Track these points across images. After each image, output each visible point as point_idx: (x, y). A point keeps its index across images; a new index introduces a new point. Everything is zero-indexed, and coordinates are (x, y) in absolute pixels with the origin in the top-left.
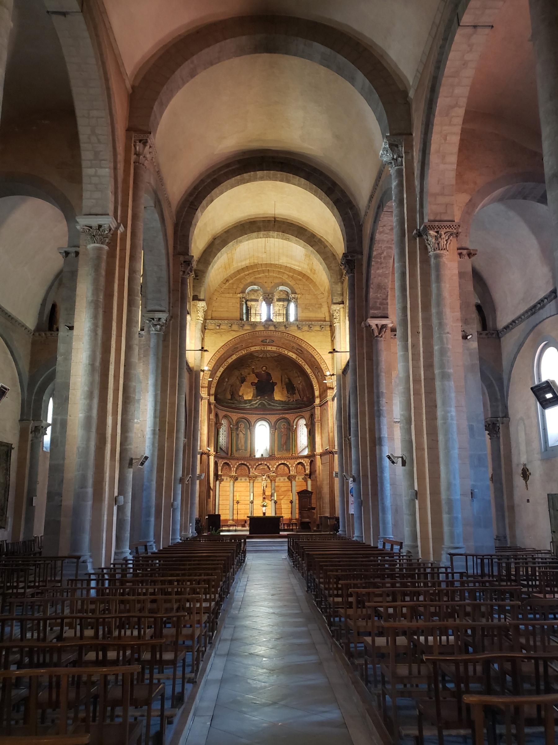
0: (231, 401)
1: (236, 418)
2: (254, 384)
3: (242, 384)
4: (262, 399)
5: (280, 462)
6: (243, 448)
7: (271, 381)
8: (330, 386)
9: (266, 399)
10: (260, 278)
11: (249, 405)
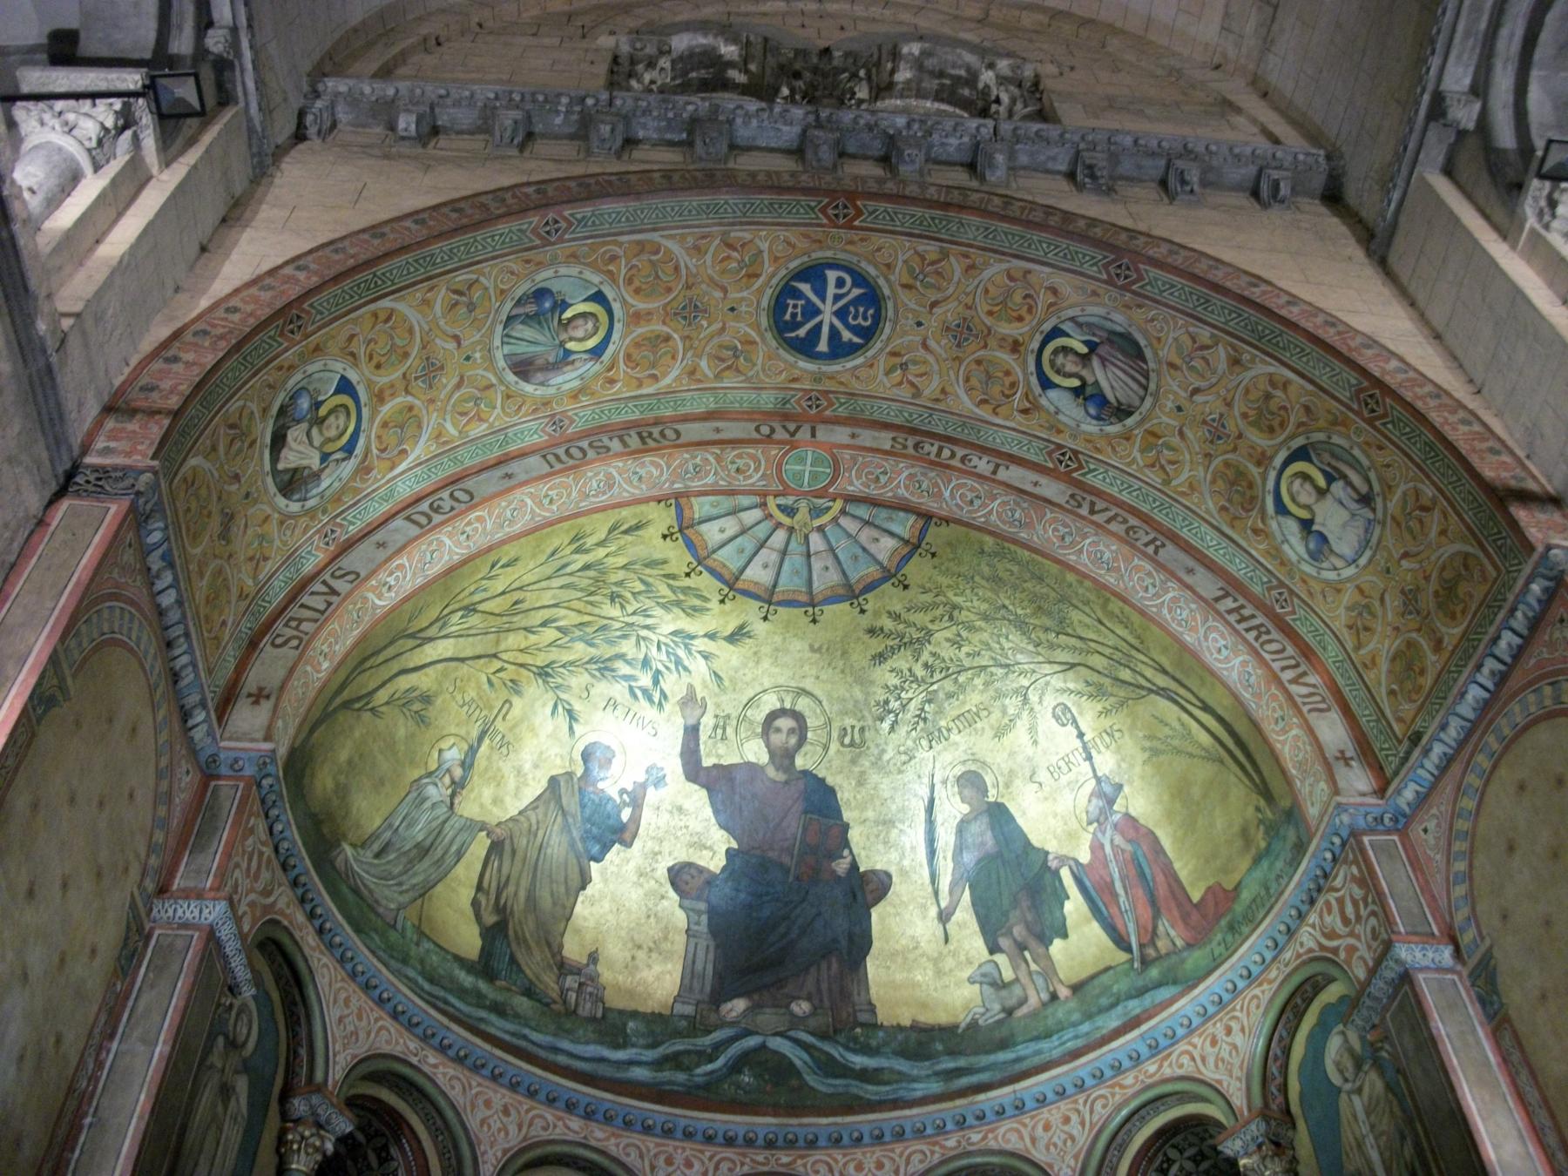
0: (483, 986)
1: (514, 1139)
4: (768, 1018)
7: (841, 866)
8: (1513, 483)
9: (796, 1022)
10: (765, 14)
11: (650, 1055)
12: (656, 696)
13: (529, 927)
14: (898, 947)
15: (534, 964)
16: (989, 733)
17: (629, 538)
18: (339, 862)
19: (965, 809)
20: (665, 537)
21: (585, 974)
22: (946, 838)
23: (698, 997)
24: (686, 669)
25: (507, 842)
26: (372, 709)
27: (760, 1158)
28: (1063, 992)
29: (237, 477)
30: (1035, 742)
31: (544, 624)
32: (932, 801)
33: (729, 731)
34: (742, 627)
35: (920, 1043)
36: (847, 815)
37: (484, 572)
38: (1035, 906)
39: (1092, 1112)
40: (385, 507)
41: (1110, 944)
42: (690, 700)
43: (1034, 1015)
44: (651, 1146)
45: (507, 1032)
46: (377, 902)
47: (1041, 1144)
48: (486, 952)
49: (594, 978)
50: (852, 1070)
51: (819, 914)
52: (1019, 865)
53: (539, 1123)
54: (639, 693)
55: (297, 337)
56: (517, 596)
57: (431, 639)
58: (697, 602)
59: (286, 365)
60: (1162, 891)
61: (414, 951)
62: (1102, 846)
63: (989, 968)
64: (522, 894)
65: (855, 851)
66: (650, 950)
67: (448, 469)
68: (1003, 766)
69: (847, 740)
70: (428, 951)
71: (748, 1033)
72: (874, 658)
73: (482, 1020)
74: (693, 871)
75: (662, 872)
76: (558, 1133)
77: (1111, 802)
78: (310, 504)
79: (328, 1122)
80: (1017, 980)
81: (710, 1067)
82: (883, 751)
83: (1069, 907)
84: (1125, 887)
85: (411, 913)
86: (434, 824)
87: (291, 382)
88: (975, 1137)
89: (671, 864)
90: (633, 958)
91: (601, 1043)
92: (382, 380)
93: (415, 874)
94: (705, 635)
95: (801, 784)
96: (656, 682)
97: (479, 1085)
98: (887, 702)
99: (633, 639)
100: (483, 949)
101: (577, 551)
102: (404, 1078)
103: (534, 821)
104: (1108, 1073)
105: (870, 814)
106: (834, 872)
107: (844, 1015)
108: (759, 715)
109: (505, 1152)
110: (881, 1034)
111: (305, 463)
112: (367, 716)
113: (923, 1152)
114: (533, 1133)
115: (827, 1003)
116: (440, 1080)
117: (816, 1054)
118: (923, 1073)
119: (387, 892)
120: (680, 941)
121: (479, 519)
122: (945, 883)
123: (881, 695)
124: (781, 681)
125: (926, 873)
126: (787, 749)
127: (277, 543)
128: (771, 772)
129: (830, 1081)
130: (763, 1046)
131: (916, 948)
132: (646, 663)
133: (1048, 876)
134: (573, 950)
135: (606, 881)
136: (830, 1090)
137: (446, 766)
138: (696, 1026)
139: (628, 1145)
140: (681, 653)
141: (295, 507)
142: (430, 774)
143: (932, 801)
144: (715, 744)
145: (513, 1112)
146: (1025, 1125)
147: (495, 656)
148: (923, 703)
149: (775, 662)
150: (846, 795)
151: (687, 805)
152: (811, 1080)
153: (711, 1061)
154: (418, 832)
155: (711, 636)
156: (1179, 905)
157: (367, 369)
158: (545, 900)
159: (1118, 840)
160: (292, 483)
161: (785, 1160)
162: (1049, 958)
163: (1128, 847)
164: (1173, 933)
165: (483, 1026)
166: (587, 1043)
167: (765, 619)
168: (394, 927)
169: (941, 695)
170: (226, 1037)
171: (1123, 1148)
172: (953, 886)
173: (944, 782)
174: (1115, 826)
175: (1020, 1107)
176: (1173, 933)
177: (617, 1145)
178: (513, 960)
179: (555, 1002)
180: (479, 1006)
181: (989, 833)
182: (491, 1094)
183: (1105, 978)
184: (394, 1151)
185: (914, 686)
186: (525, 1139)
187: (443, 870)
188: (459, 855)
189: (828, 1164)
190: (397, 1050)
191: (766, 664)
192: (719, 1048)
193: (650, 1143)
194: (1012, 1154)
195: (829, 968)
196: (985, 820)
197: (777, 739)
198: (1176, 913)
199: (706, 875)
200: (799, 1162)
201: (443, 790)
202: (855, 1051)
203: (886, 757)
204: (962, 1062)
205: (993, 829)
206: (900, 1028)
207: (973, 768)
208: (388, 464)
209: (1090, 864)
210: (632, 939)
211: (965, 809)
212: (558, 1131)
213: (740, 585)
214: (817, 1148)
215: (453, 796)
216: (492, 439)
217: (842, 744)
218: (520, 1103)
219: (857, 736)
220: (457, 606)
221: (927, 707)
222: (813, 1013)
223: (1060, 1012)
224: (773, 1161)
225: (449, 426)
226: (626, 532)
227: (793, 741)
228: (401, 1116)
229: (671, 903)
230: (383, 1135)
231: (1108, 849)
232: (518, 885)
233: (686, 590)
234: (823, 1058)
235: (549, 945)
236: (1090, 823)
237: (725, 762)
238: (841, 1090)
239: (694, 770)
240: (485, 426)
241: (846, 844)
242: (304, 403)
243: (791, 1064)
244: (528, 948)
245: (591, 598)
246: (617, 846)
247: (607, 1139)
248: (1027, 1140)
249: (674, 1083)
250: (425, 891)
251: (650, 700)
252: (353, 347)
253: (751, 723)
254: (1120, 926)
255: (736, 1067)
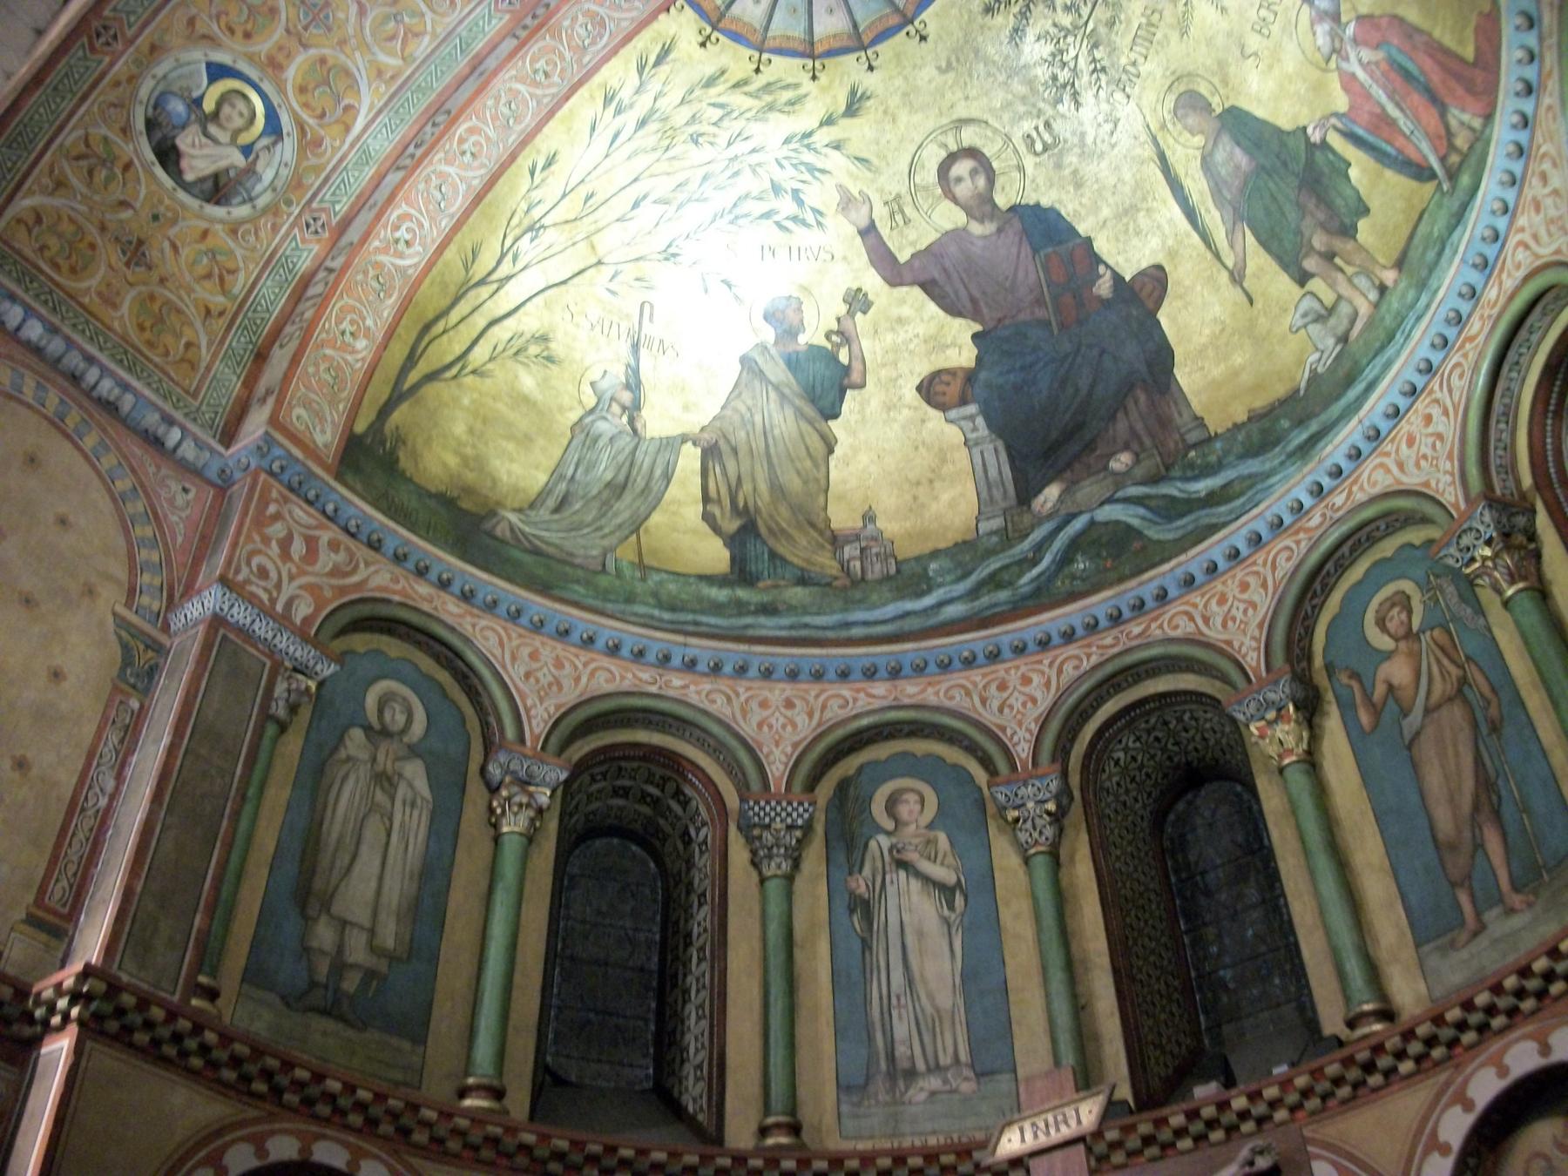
0: (742, 593)
1: (805, 727)
2: (955, 389)
3: (835, 426)
4: (1090, 490)
5: (1485, 1087)
6: (954, 1042)
7: (1104, 287)
9: (1121, 479)
12: (810, 219)
13: (784, 514)
14: (1203, 340)
15: (801, 550)
16: (1174, 36)
17: (664, 69)
18: (501, 530)
19: (1199, 140)
20: (703, 45)
21: (867, 538)
22: (1197, 186)
23: (1003, 505)
24: (823, 171)
25: (722, 443)
26: (474, 372)
27: (1109, 641)
28: (1389, 276)
29: (124, 204)
30: (1224, 10)
31: (636, 205)
32: (1162, 157)
33: (909, 210)
34: (853, 92)
35: (1264, 432)
36: (1082, 229)
37: (525, 183)
38: (1324, 200)
39: (1450, 391)
40: (369, 172)
41: (1413, 184)
42: (847, 202)
43: (1370, 324)
44: (978, 679)
45: (782, 628)
46: (572, 555)
47: (1410, 466)
48: (739, 562)
49: (877, 538)
50: (1199, 499)
51: (1103, 352)
52: (1285, 164)
53: (834, 704)
54: (789, 224)
55: (119, 46)
56: (583, 191)
57: (509, 278)
58: (788, 95)
59: (123, 78)
60: (1436, 78)
61: (639, 588)
62: (1353, 76)
63: (1308, 303)
64: (763, 487)
65: (1111, 262)
66: (931, 481)
67: (418, 105)
68: (1209, 62)
69: (1039, 147)
70: (661, 583)
71: (1072, 517)
72: (1012, 38)
73: (747, 627)
74: (945, 378)
75: (910, 394)
76: (863, 703)
77: (1335, 17)
78: (261, 202)
79: (530, 776)
80: (1340, 297)
81: (1035, 572)
82: (1083, 135)
83: (1353, 173)
84: (1398, 105)
85: (627, 553)
86: (621, 458)
87: (144, 93)
88: (1339, 499)
89: (917, 382)
90: (915, 498)
91: (902, 598)
92: (263, 46)
93: (616, 515)
94: (821, 125)
95: (1017, 224)
96: (800, 203)
97: (748, 689)
98: (1055, 78)
99: (748, 171)
100: (733, 559)
101: (618, 112)
102: (646, 710)
103: (743, 409)
104: (1451, 333)
105: (1106, 212)
106: (1099, 299)
107: (1172, 445)
108: (929, 175)
109: (795, 745)
110: (1218, 445)
111: (222, 164)
112: (469, 380)
113: (1288, 548)
114: (828, 714)
115: (1147, 442)
116: (694, 699)
117: (1153, 503)
118: (1276, 462)
119: (581, 541)
120: (962, 458)
121: (471, 131)
122: (1220, 235)
123: (1042, 73)
124: (931, 124)
125: (1196, 238)
126: (980, 195)
127: (239, 253)
128: (977, 229)
129: (1179, 523)
130: (1092, 523)
131: (1223, 330)
132: (776, 189)
133: (1319, 157)
134: (842, 517)
135: (854, 433)
136: (1180, 533)
137: (608, 396)
138: (1007, 537)
139: (947, 691)
140: (808, 157)
141: (242, 211)
142: (592, 411)
143: (1162, 157)
144: (901, 233)
145: (797, 702)
146: (1387, 454)
147: (600, 263)
148: (1090, 52)
149: (913, 110)
150: (1070, 207)
151: (906, 311)
152: (1153, 533)
153: (1034, 562)
154: (604, 470)
155: (828, 121)
156: (1458, 77)
157: (238, 44)
158: (793, 483)
159: (1367, 54)
160: (218, 189)
161: (1137, 630)
162: (1361, 248)
163: (1380, 55)
164: (1466, 117)
165: (750, 632)
166: (884, 604)
167: (871, 68)
168: (604, 569)
169: (1102, 30)
170: (368, 729)
171: (1510, 414)
172: (1230, 234)
173: (1163, 126)
174: (1355, 41)
175: (1375, 436)
176: (1466, 117)
177: (937, 693)
178: (774, 555)
179: (836, 578)
180: (740, 614)
181: (1238, 151)
182: (766, 693)
183: (1422, 229)
184: (688, 791)
185: (1070, 39)
186: (819, 725)
187: (652, 497)
188: (668, 477)
189: (1186, 613)
190: (626, 685)
191: (903, 117)
192: (1040, 549)
193: (977, 676)
194: (1386, 495)
195: (1136, 402)
196: (1226, 139)
197: (963, 190)
198: (1460, 91)
199: (961, 375)
200: (1154, 626)
201: (617, 421)
202: (1196, 478)
203: (1089, 140)
204: (1314, 427)
205: (1238, 144)
206: (1237, 427)
207: (1182, 88)
208: (337, 129)
209: (1351, 108)
210: (907, 479)
211: (1199, 140)
212: (860, 703)
213: (819, 49)
214: (1170, 602)
215: (631, 421)
216: (446, 50)
217: (1036, 154)
218: (807, 691)
219: (1047, 138)
220: (517, 232)
221: (1098, 54)
222: (1137, 460)
223: (1394, 302)
224: (1123, 638)
225: (383, 58)
226: (658, 63)
227: (981, 182)
228: (674, 753)
229: (942, 429)
230: (669, 779)
231: (1361, 75)
232: (754, 480)
233: (768, 88)
234: (1161, 503)
235: (813, 525)
236: (1328, 60)
237: (922, 245)
238: (1190, 528)
239: (893, 272)
240: (427, 39)
241: (1098, 260)
242: (177, 107)
243: (1129, 527)
244: (789, 537)
245: (671, 153)
246: (849, 393)
247: (923, 691)
248: (1395, 469)
249: (995, 605)
250: (636, 525)
251: (804, 223)
252: (201, 28)
253: (926, 188)
254: (1414, 156)
255: (1066, 559)
